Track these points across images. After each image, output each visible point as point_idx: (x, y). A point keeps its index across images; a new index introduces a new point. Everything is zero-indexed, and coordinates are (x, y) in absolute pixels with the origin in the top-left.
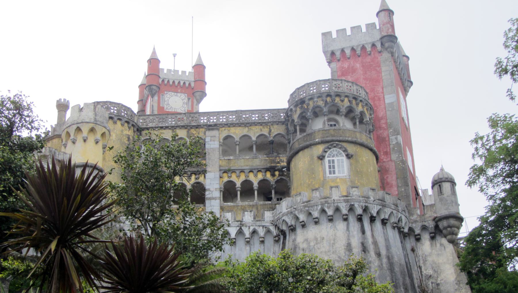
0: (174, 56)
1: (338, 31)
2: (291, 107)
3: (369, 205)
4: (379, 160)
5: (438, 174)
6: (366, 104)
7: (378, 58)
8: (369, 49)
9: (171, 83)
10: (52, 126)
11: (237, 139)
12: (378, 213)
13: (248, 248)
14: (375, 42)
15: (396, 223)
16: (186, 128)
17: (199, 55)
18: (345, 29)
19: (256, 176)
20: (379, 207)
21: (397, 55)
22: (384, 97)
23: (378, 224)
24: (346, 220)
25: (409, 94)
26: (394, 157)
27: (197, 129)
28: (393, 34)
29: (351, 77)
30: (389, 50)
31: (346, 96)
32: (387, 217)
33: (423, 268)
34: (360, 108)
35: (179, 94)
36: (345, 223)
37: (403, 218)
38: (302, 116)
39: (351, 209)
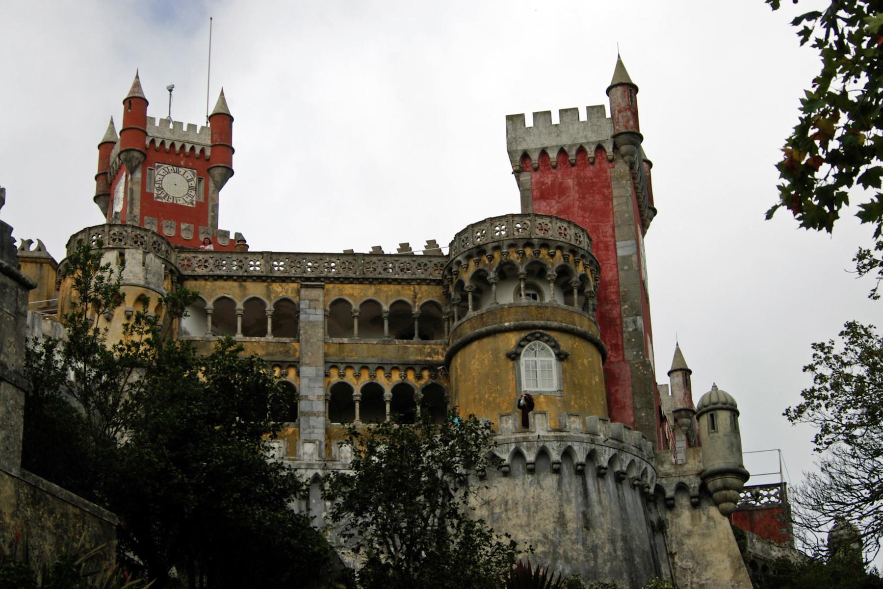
0: (170, 91)
1: (535, 115)
2: (459, 258)
3: (597, 448)
4: (607, 361)
5: (710, 394)
6: (591, 262)
8: (591, 151)
9: (167, 147)
11: (355, 306)
12: (611, 461)
14: (604, 141)
15: (638, 479)
16: (264, 281)
17: (222, 93)
19: (389, 377)
20: (613, 452)
21: (637, 166)
22: (615, 245)
23: (610, 481)
24: (557, 471)
25: (649, 231)
26: (630, 354)
27: (284, 284)
28: (634, 130)
29: (558, 202)
30: (626, 158)
31: (560, 248)
32: (624, 469)
34: (580, 269)
35: (182, 170)
36: (555, 477)
37: (650, 469)
38: (480, 277)
39: (568, 453)
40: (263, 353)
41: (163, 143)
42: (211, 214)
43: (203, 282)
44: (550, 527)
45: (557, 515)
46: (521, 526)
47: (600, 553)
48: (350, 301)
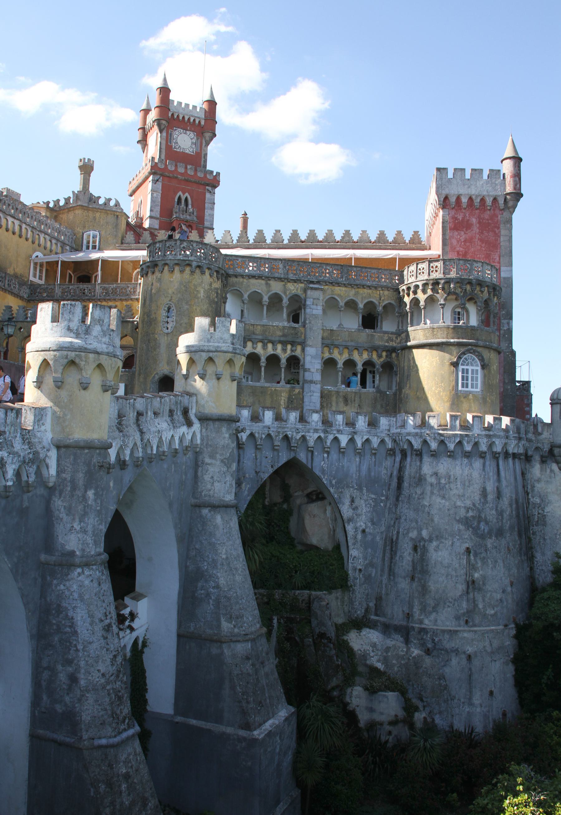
2: (417, 283)
7: (497, 217)
9: (181, 118)
10: (73, 192)
11: (342, 304)
13: (358, 459)
14: (499, 196)
16: (283, 281)
18: (464, 170)
19: (361, 355)
24: (483, 458)
27: (295, 284)
29: (465, 233)
33: (530, 495)
35: (188, 132)
36: (481, 461)
40: (281, 334)
41: (178, 116)
42: (203, 159)
43: (241, 280)
44: (477, 498)
45: (482, 489)
46: (459, 496)
47: (505, 516)
48: (339, 299)
